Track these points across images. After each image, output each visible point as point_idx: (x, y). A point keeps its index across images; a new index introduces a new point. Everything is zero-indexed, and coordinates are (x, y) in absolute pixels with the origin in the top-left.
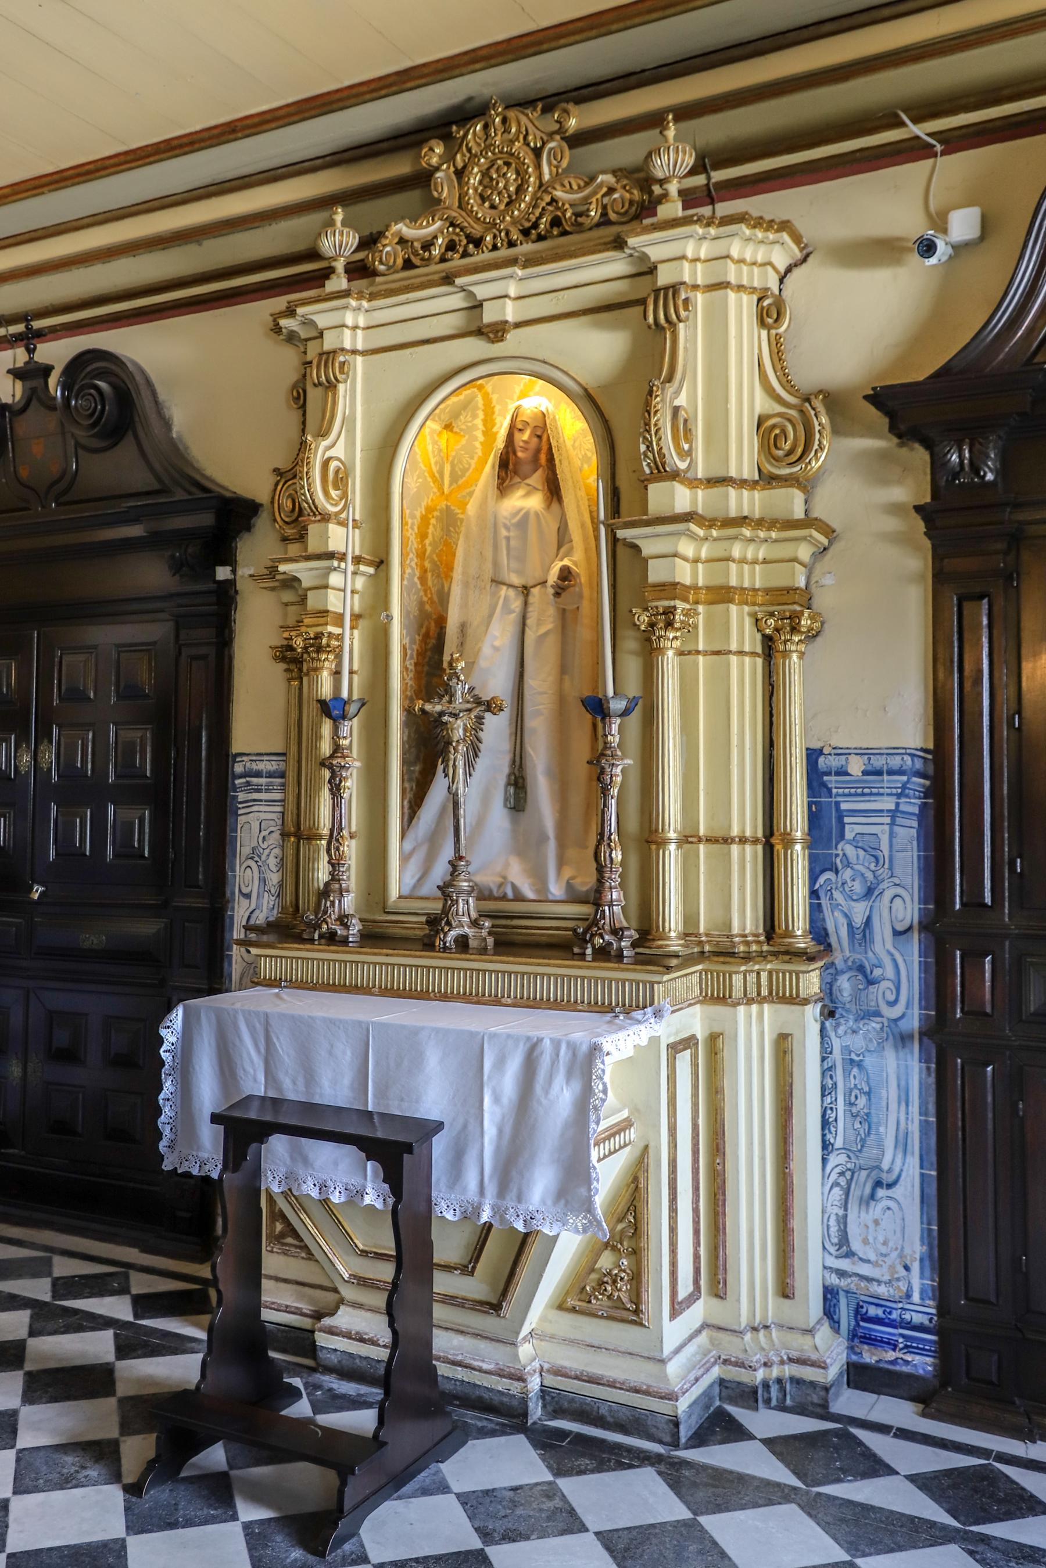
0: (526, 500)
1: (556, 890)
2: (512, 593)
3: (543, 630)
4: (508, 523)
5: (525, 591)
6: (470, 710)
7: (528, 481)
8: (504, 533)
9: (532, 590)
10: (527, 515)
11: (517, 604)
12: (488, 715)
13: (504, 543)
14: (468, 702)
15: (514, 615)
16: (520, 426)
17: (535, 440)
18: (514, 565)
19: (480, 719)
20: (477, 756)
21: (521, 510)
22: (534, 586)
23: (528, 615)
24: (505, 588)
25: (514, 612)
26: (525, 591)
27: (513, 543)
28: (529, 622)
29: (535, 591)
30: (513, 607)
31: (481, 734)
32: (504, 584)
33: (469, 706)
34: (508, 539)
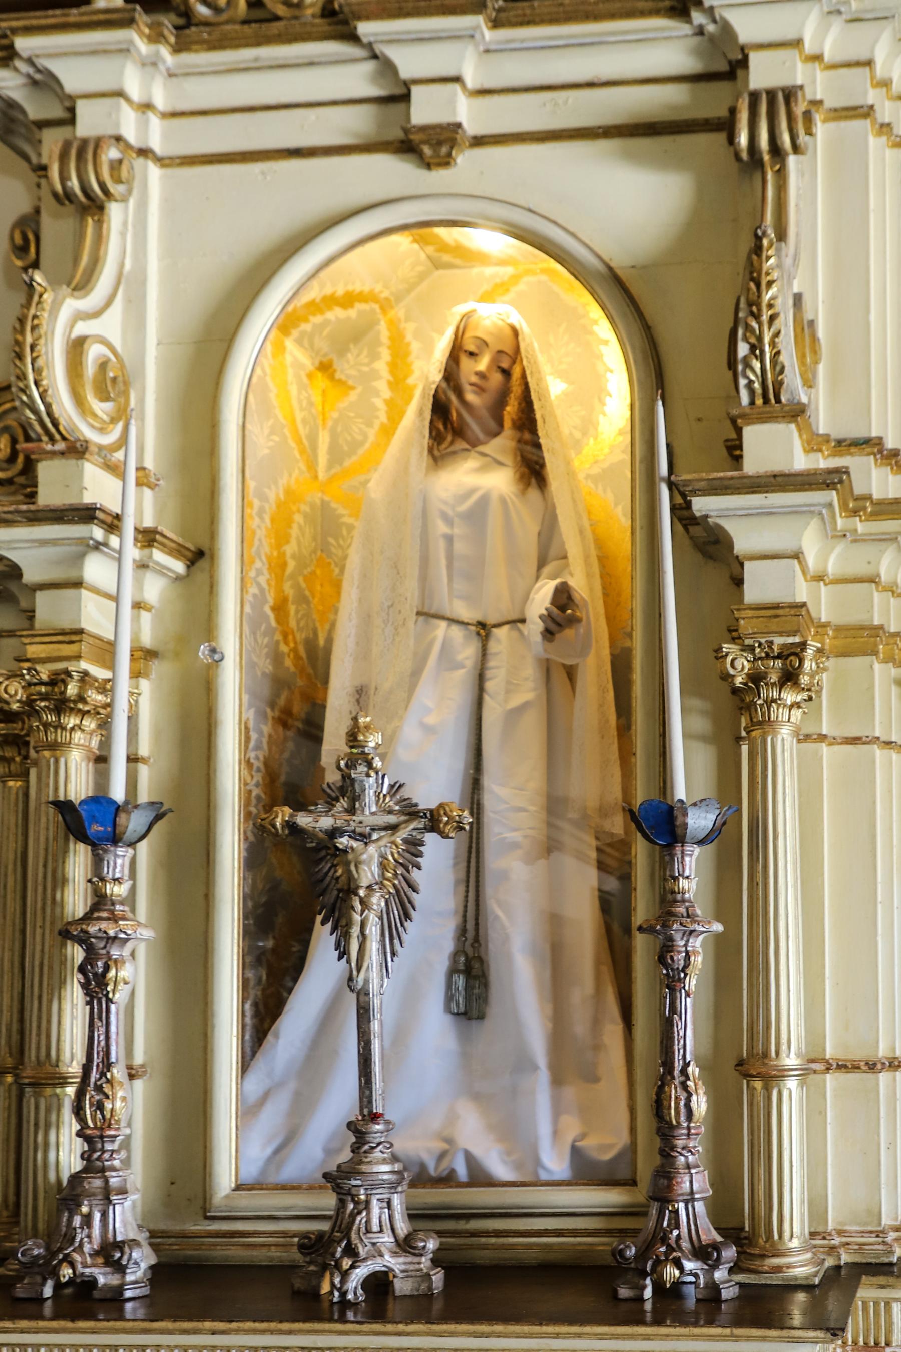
0: (482, 475)
1: (556, 1164)
2: (456, 632)
3: (516, 701)
4: (450, 512)
5: (483, 630)
6: (393, 828)
7: (481, 448)
8: (442, 528)
9: (494, 630)
10: (484, 500)
11: (468, 653)
12: (431, 838)
13: (442, 544)
14: (390, 812)
15: (461, 672)
16: (471, 347)
17: (496, 378)
18: (460, 585)
19: (414, 846)
20: (408, 916)
21: (472, 491)
22: (498, 625)
23: (488, 674)
24: (443, 624)
25: (463, 667)
26: (483, 630)
27: (459, 547)
28: (489, 685)
29: (501, 633)
30: (460, 657)
31: (415, 874)
32: (443, 618)
33: (392, 819)
34: (449, 539)
